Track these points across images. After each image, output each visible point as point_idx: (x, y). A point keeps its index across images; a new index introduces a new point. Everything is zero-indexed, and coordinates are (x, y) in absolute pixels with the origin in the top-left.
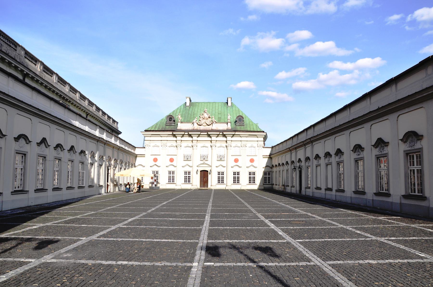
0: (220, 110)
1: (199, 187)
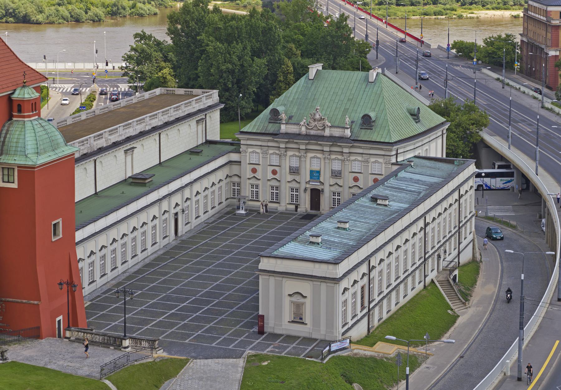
1: (309, 210)
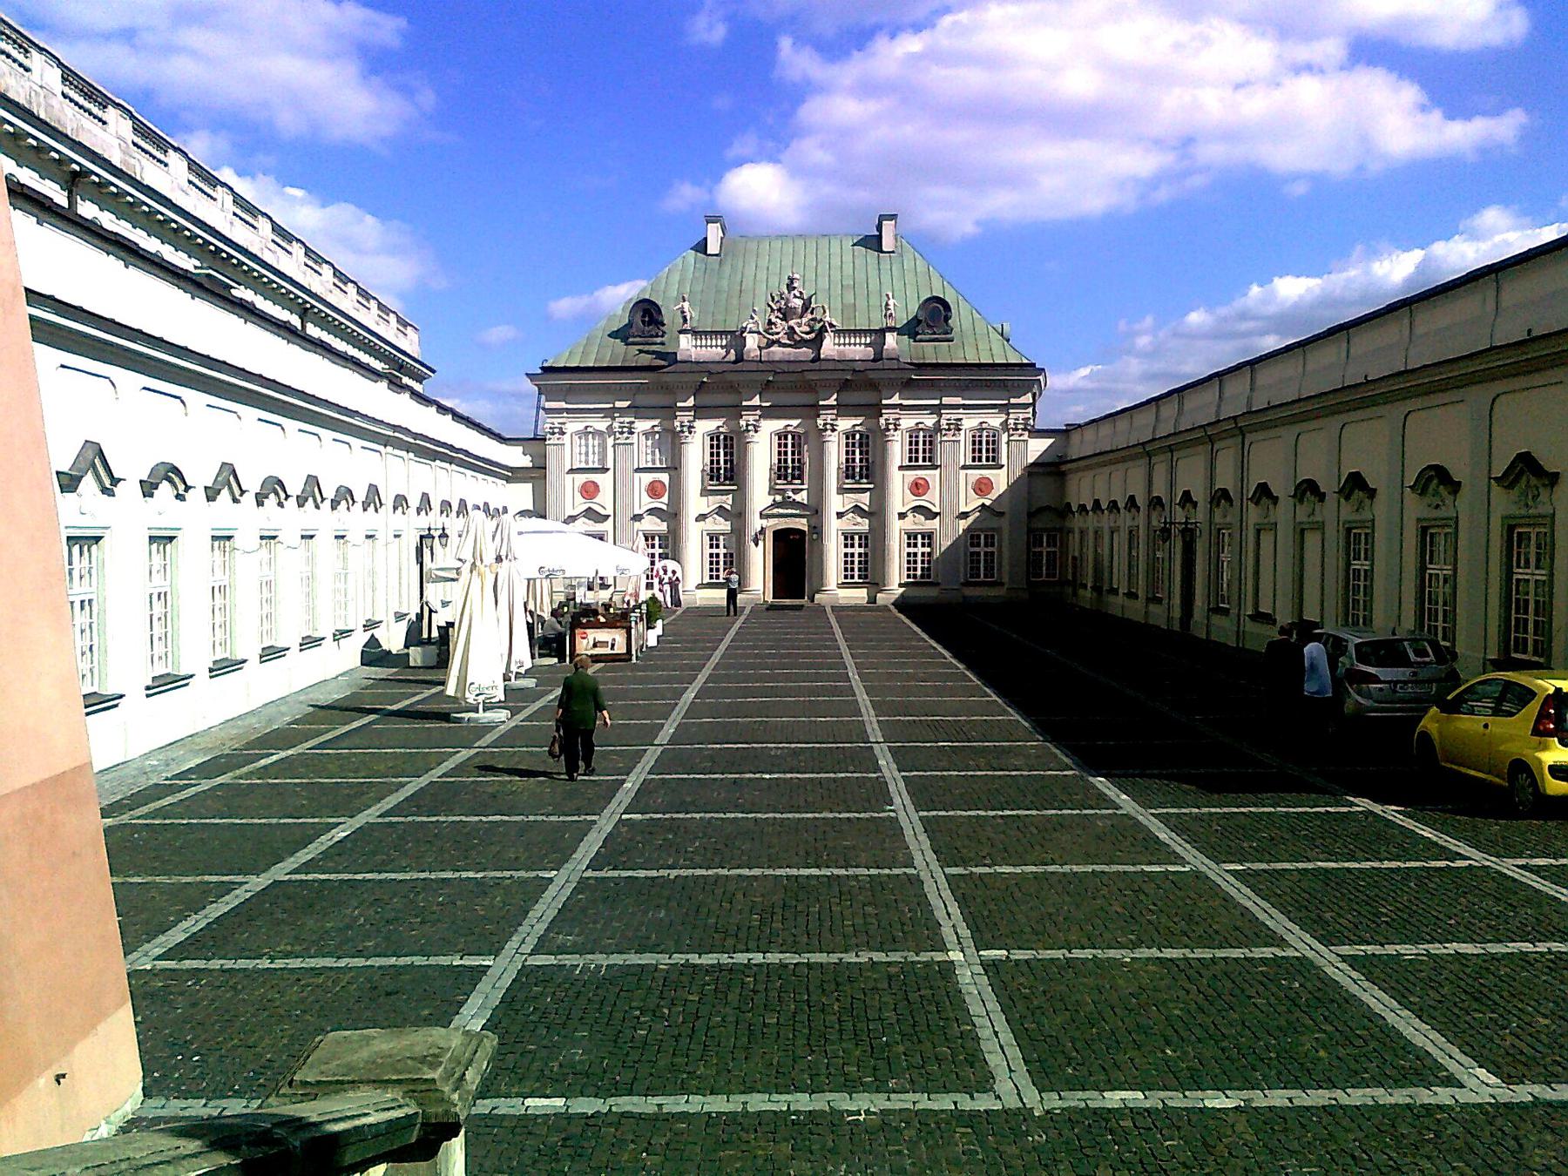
0: (848, 269)
1: (769, 598)
